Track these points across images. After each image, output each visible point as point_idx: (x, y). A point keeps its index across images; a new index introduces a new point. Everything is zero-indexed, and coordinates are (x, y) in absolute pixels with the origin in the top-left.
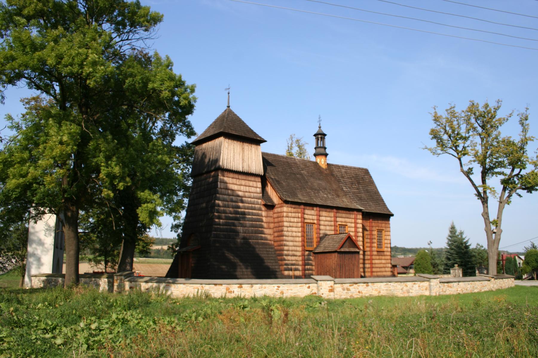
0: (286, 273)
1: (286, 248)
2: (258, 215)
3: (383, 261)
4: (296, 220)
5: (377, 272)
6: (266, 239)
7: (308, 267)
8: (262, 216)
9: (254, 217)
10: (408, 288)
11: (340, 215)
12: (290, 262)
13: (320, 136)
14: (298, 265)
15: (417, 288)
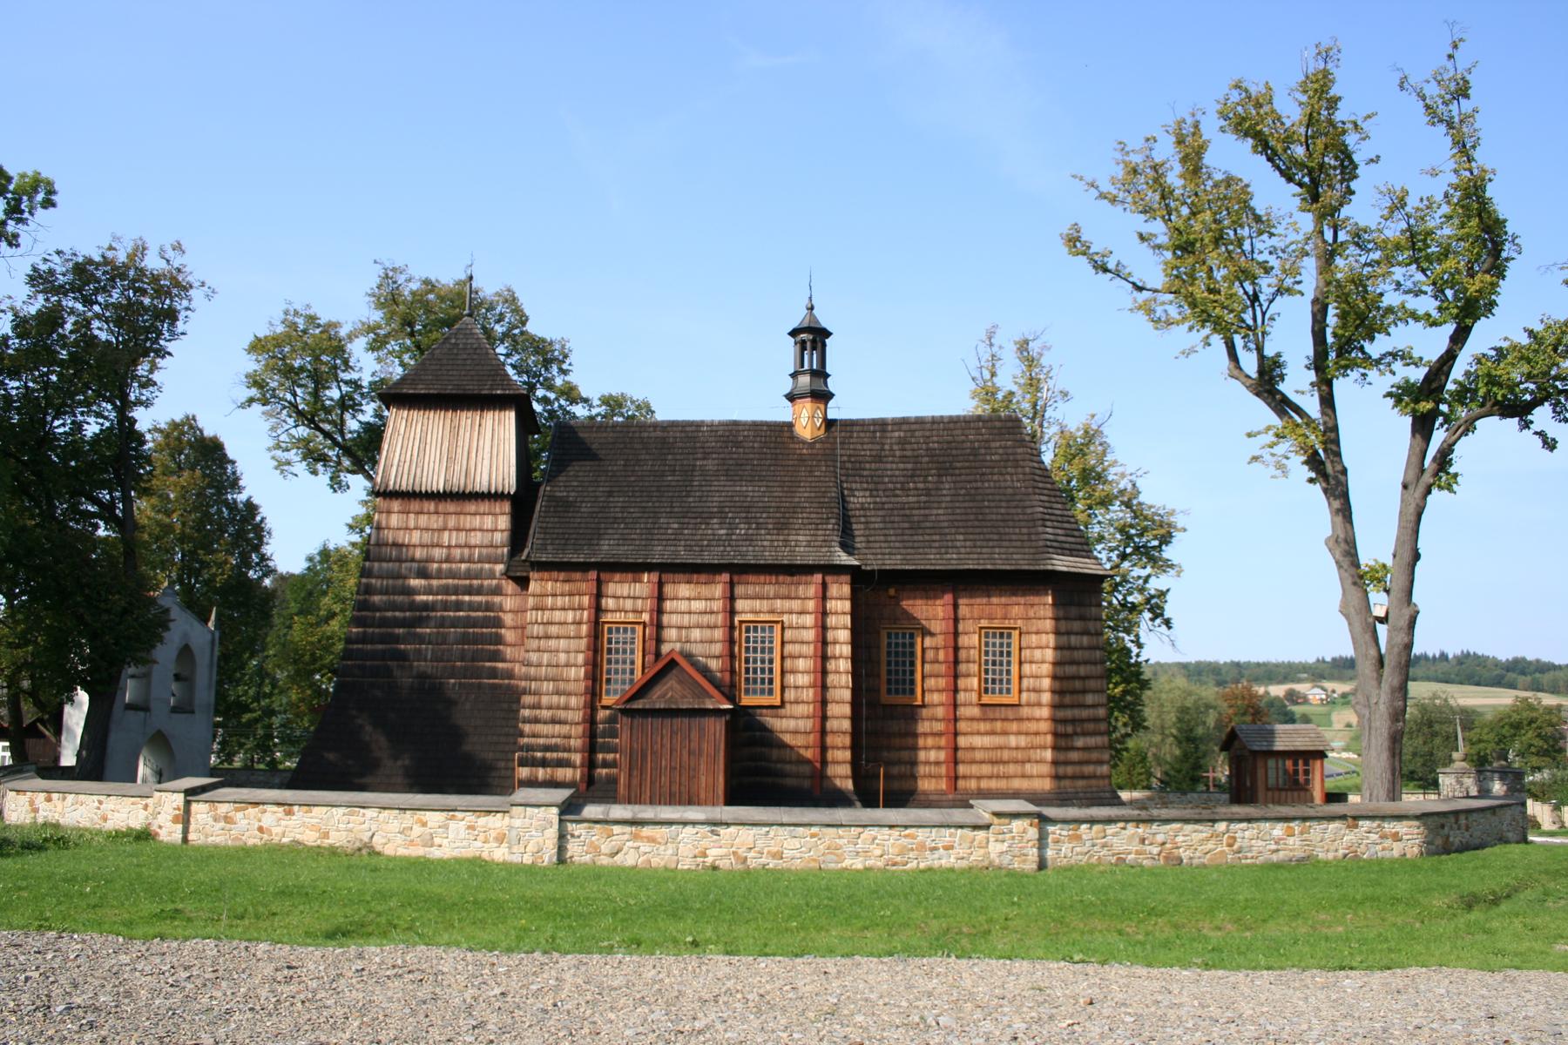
0: (524, 772)
1: (527, 699)
2: (489, 607)
3: (1013, 741)
4: (570, 616)
5: (979, 778)
6: (510, 675)
7: (610, 756)
8: (501, 610)
9: (473, 614)
10: (427, 830)
11: (751, 590)
12: (541, 741)
13: (812, 337)
14: (569, 750)
15: (463, 833)
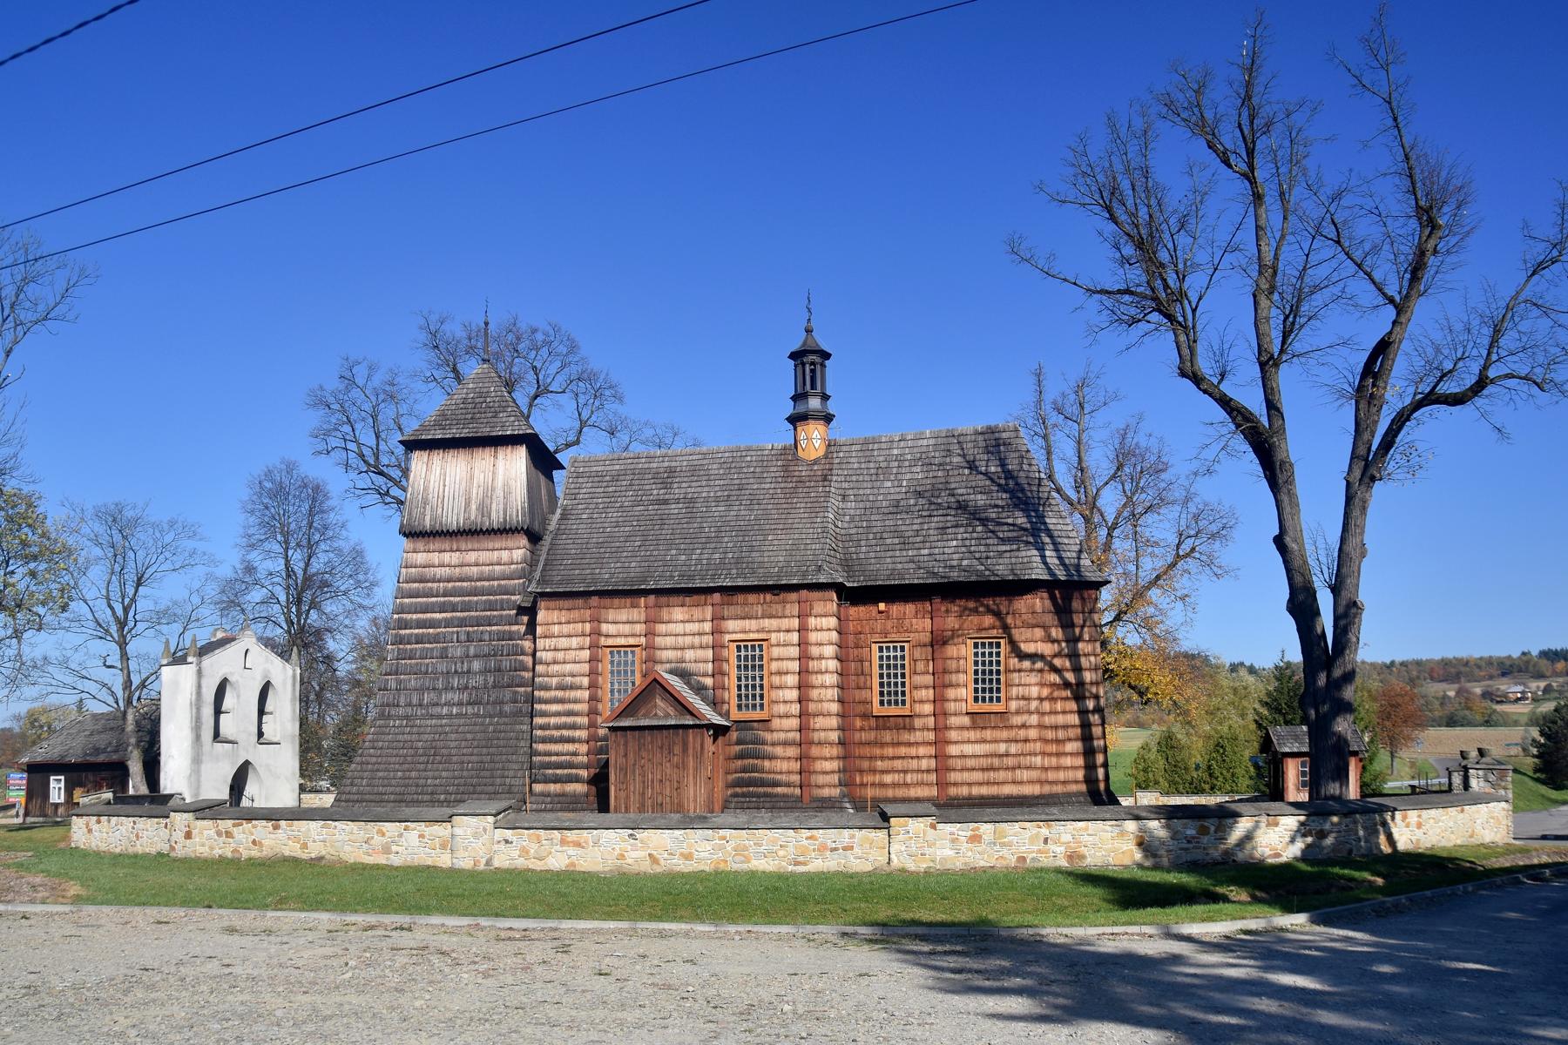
4: (574, 642)
5: (970, 784)
